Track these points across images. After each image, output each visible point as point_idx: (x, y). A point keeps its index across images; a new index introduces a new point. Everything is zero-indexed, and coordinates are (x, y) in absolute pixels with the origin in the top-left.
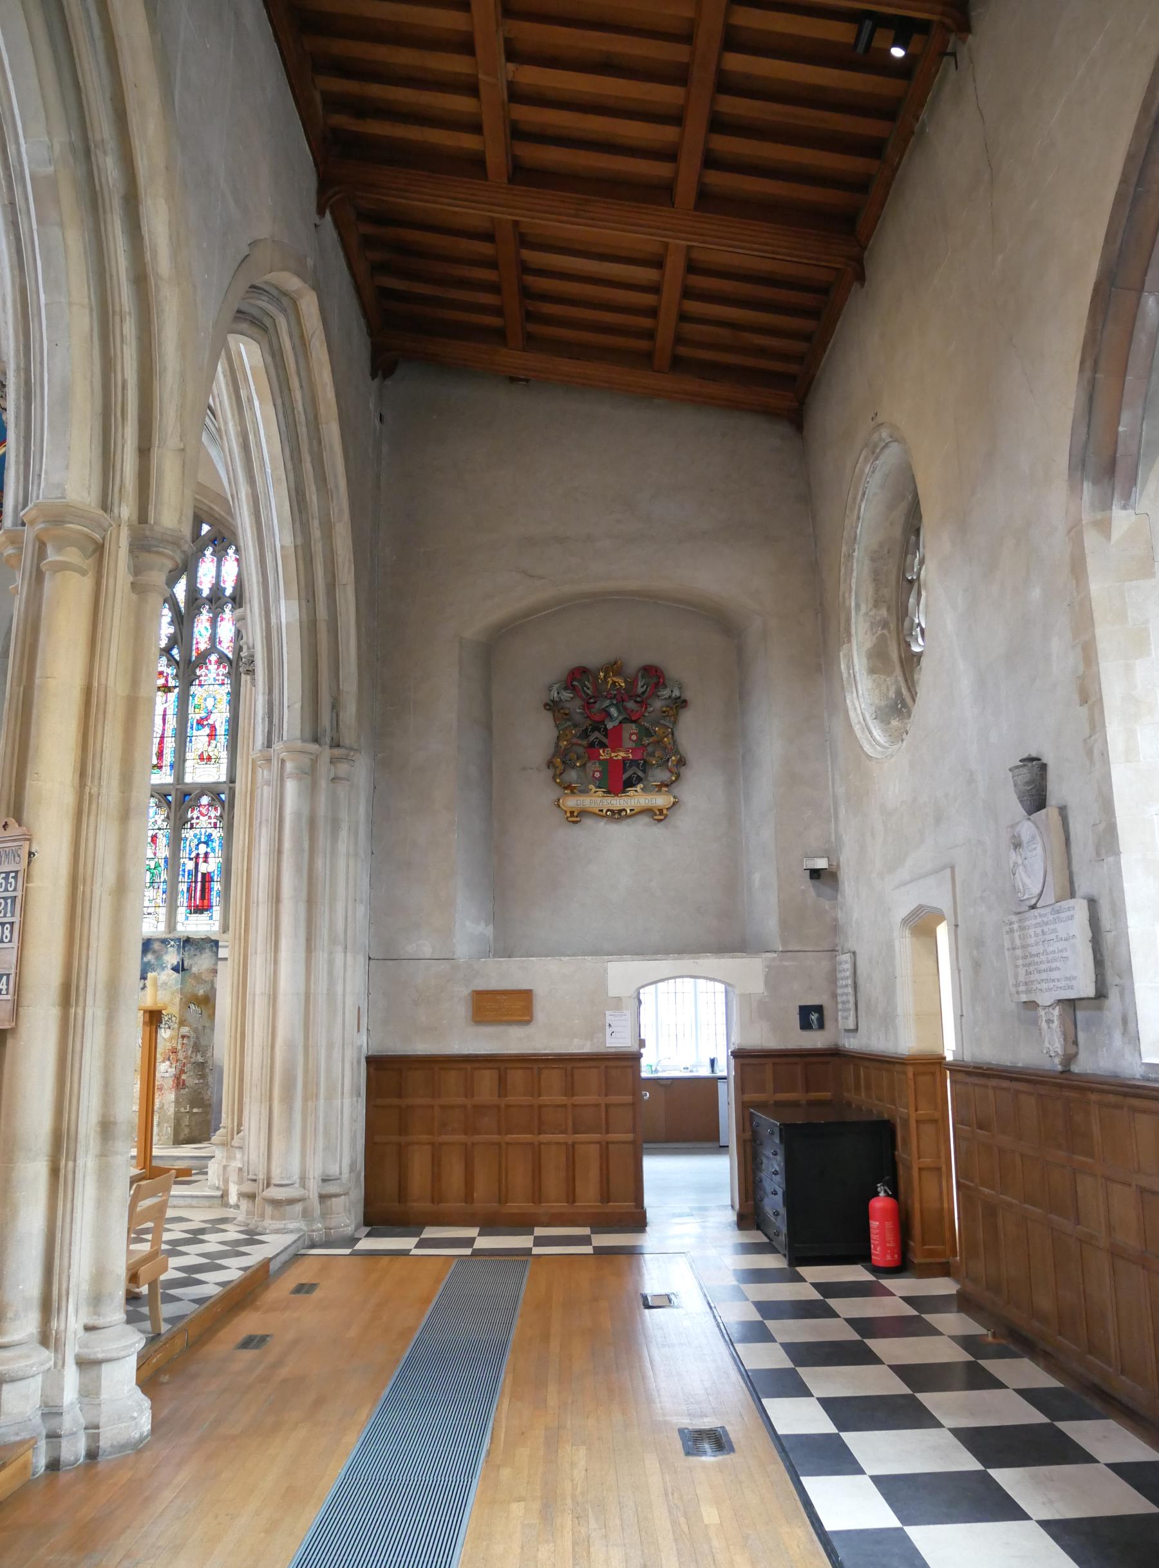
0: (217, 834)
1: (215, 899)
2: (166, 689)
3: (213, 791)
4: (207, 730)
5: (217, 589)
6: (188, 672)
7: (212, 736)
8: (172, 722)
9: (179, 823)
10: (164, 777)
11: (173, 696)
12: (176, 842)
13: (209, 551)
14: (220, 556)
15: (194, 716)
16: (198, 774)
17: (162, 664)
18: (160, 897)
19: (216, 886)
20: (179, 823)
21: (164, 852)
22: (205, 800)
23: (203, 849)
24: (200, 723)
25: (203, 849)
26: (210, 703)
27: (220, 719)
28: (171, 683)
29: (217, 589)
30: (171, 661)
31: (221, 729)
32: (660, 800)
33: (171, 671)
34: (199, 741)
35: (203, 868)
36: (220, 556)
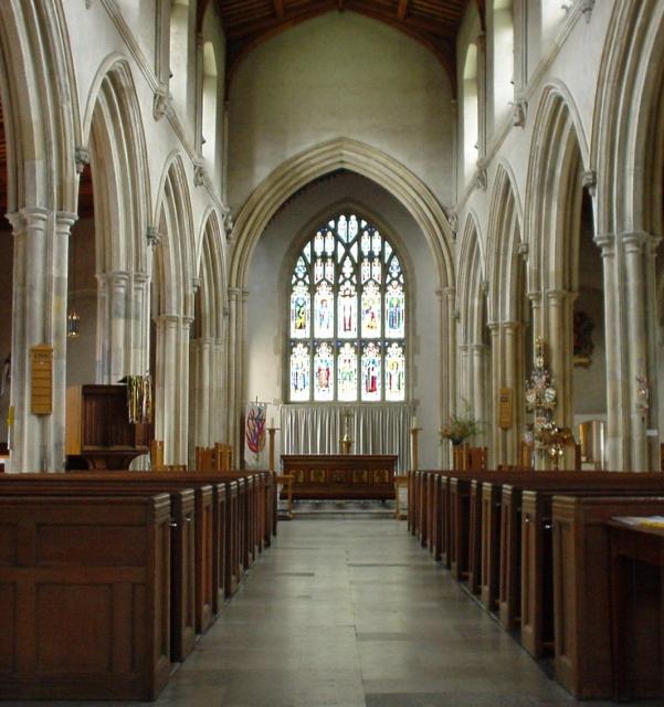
0: (379, 358)
1: (379, 387)
2: (351, 296)
3: (375, 341)
4: (370, 315)
5: (371, 254)
6: (360, 289)
7: (373, 317)
8: (355, 310)
9: (360, 352)
10: (353, 335)
11: (355, 298)
12: (360, 361)
13: (366, 233)
14: (371, 234)
15: (364, 308)
16: (366, 334)
17: (348, 284)
18: (354, 385)
19: (378, 381)
20: (360, 352)
21: (354, 365)
22: (371, 345)
23: (371, 366)
24: (367, 312)
25: (371, 366)
26: (371, 303)
27: (377, 308)
28: (353, 293)
29: (371, 254)
30: (352, 283)
31: (377, 313)
32: (584, 360)
33: (353, 288)
34: (366, 319)
35: (372, 374)
36: (371, 234)
